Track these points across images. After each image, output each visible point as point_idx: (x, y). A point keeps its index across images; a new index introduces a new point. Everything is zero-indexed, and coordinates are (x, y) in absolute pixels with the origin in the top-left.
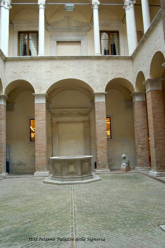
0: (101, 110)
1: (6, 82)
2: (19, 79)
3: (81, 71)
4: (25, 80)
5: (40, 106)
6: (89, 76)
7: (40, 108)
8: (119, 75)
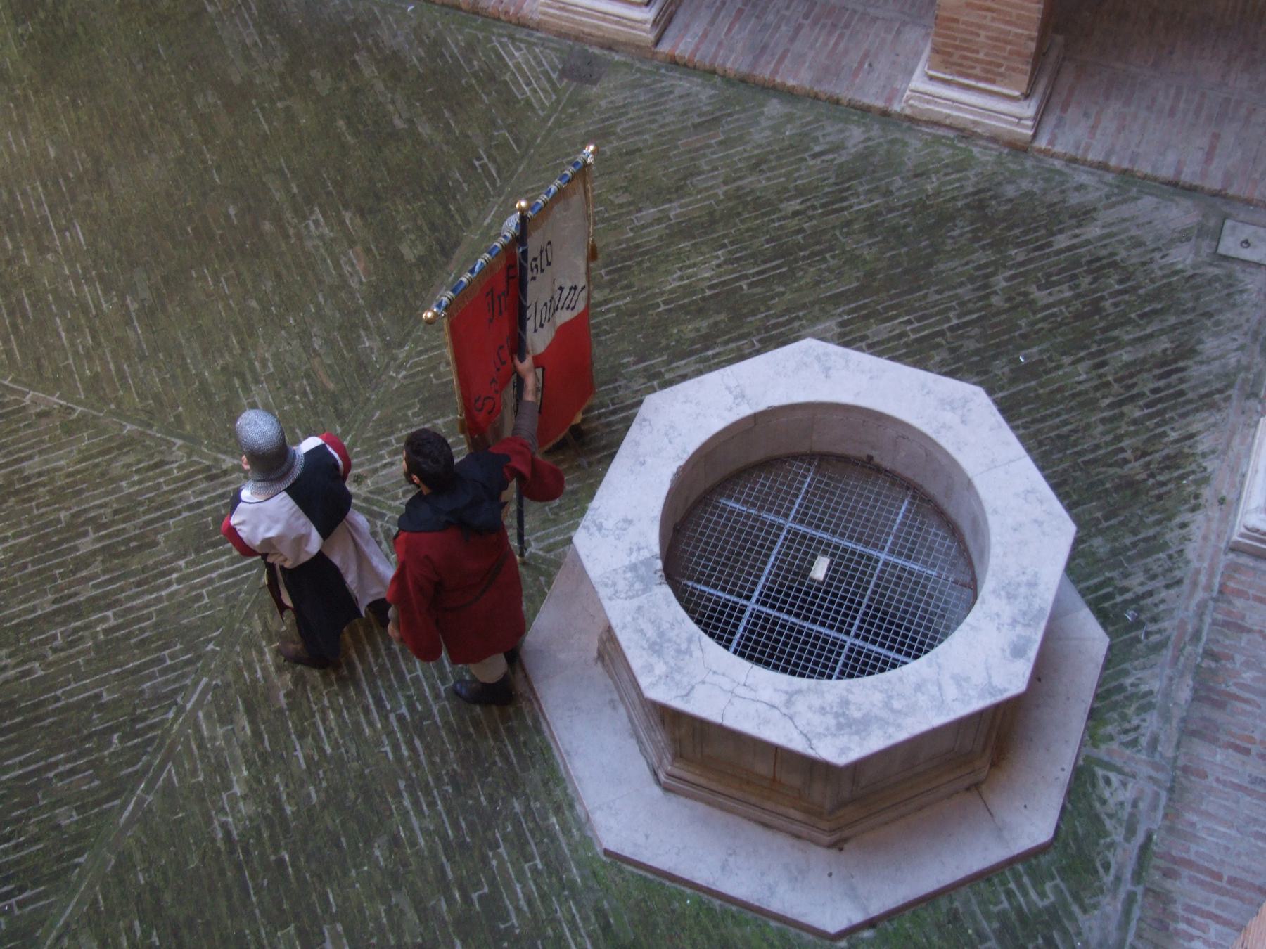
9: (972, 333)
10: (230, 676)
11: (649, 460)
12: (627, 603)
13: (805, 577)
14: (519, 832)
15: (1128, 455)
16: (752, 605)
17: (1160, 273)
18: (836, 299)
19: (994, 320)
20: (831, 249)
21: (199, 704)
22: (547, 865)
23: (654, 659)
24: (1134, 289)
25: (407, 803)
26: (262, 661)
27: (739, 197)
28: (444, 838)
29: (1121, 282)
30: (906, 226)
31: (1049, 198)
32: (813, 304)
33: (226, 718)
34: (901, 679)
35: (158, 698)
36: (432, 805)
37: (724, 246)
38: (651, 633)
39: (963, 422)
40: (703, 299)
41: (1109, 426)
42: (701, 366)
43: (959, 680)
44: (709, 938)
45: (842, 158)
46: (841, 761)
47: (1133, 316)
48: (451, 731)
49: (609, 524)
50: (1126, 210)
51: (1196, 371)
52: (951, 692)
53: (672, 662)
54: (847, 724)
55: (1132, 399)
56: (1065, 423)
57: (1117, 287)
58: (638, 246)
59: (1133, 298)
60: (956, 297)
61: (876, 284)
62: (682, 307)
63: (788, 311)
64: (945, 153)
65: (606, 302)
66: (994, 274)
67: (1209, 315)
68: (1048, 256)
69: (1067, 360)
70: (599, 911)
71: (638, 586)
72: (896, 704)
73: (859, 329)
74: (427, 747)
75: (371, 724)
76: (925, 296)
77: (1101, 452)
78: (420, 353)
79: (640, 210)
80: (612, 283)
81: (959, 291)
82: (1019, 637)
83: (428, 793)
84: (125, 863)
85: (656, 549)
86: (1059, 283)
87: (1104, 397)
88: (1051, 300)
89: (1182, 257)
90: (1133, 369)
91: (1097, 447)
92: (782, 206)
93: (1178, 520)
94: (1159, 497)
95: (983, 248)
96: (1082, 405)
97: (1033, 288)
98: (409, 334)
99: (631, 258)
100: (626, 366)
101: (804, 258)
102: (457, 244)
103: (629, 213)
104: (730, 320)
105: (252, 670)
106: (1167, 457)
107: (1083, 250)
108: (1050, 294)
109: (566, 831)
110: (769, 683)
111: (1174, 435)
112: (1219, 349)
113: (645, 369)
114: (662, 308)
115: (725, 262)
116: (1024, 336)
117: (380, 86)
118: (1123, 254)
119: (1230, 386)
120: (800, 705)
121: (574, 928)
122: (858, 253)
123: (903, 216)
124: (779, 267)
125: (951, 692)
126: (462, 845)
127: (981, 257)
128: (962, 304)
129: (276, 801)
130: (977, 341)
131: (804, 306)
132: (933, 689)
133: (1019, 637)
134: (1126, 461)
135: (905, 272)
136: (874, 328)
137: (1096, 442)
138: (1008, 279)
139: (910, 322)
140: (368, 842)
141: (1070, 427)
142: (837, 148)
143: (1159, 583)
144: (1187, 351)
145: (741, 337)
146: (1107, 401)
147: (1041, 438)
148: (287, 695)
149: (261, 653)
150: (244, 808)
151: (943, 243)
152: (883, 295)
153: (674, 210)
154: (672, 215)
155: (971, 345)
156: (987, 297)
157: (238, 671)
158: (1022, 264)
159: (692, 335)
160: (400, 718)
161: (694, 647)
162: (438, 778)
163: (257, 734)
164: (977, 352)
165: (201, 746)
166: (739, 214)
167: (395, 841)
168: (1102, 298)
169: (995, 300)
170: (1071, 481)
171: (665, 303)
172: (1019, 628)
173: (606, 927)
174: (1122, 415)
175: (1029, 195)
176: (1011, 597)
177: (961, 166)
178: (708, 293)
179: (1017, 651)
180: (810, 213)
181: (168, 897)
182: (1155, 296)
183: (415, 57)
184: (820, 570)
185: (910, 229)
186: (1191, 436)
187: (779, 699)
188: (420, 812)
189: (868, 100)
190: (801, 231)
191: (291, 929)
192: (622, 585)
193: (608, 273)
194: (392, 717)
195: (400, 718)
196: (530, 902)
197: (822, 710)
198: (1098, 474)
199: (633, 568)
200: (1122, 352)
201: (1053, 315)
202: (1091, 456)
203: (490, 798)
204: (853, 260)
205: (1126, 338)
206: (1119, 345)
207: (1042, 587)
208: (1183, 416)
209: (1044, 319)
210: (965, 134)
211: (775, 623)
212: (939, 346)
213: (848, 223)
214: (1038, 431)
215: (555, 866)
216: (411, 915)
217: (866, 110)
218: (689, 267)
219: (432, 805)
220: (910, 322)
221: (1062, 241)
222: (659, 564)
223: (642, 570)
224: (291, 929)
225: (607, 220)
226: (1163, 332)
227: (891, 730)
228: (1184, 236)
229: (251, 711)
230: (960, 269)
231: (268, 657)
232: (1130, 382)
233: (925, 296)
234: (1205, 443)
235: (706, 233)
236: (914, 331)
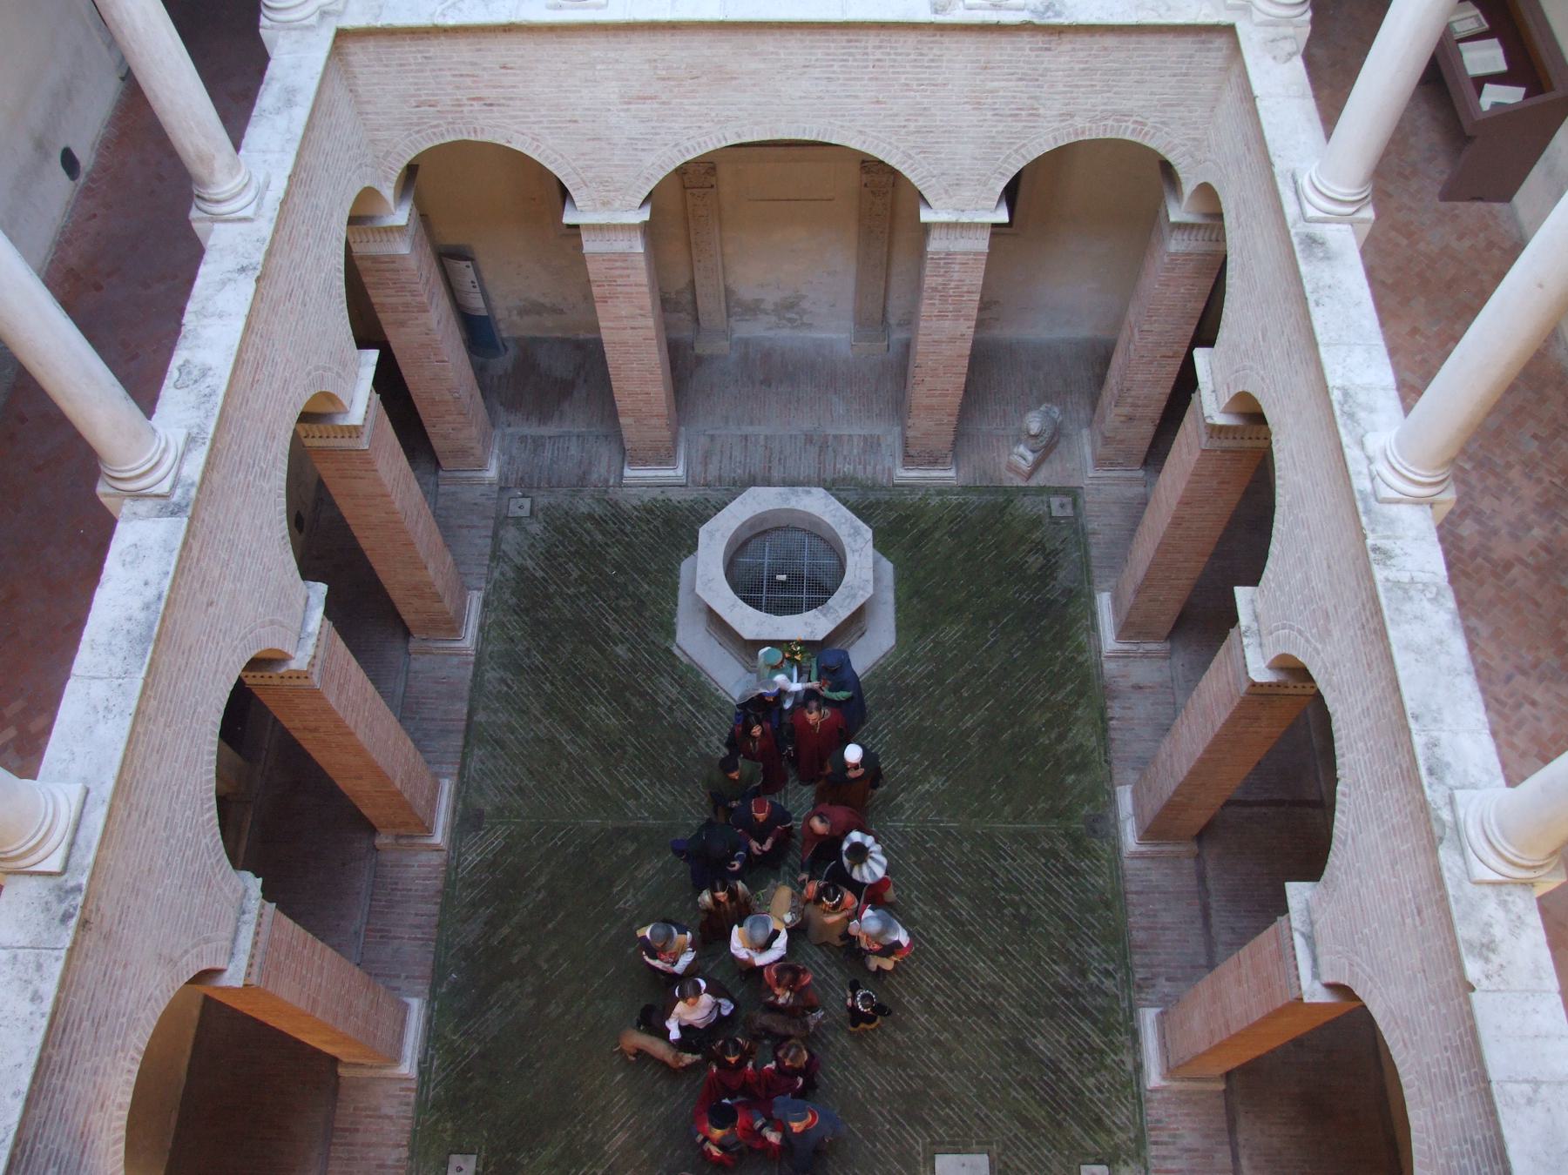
0: (953, 284)
1: (388, 153)
2: (466, 137)
3: (856, 97)
4: (503, 142)
5: (618, 264)
6: (912, 126)
7: (617, 272)
8: (1110, 122)
18: (602, 651)
31: (513, 584)
33: (901, 806)
45: (509, 676)
50: (512, 554)
51: (599, 511)
54: (857, 532)
63: (615, 668)
64: (493, 634)
89: (535, 528)
112: (584, 505)
117: (516, 919)
127: (558, 601)
142: (503, 681)
144: (590, 517)
150: (933, 779)
153: (564, 737)
155: (612, 593)
167: (921, 719)
175: (513, 594)
177: (502, 625)
182: (564, 535)
183: (485, 912)
184: (783, 577)
189: (470, 673)
210: (481, 628)
213: (552, 661)
215: (906, 661)
216: (946, 701)
217: (475, 675)
221: (539, 574)
228: (523, 530)
234: (636, 502)
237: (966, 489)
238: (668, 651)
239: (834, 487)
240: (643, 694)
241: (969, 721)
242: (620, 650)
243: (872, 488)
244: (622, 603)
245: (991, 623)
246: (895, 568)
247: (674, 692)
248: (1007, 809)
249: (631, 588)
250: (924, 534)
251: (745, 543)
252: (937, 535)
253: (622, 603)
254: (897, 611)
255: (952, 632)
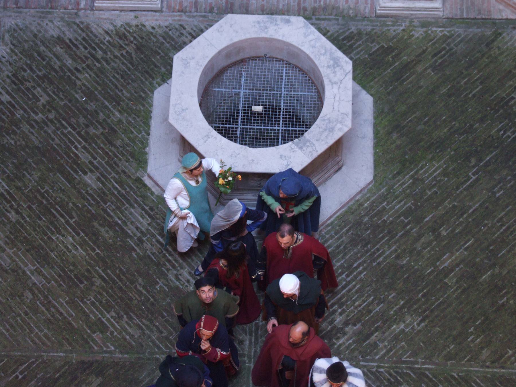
9: (75, 121)
10: (356, 353)
11: (250, 159)
12: (317, 145)
13: (262, 114)
14: (376, 215)
15: (124, 52)
16: (281, 128)
17: (15, 57)
19: (64, 114)
20: (38, 191)
21: (373, 360)
22: (384, 201)
23: (336, 129)
24: (27, 65)
25: (381, 259)
26: (344, 343)
27: (13, 241)
28: (389, 240)
29: (25, 71)
30: (13, 163)
32: (75, 188)
33: (375, 345)
34: (313, 53)
35: (378, 379)
36: (378, 250)
37: (49, 238)
38: (326, 133)
39: (193, 58)
40: (87, 235)
41: (110, 61)
42: (129, 223)
43: (306, 35)
44: (388, 139)
46: (351, 63)
47: (44, 63)
48: (345, 255)
49: (285, 163)
51: (69, 35)
52: (311, 37)
53: (335, 123)
54: (336, 63)
55: (93, 56)
56: (114, 77)
57: (29, 71)
58: (60, 276)
59: (34, 64)
60: (54, 132)
61: (56, 166)
62: (94, 243)
63: (84, 198)
65: (101, 277)
66: (35, 121)
67: (35, 36)
68: (17, 102)
69: (79, 83)
70: (394, 177)
71: (308, 144)
72: (323, 51)
73: (87, 166)
74: (356, 261)
75: (354, 286)
76: (57, 145)
77: (125, 61)
78: (159, 348)
79: (35, 284)
80: (88, 279)
81: (50, 132)
82: (281, 22)
83: (374, 253)
84: (449, 357)
85: (290, 143)
86: (33, 94)
87: (95, 65)
88: (45, 96)
90: (75, 58)
91: (123, 63)
92: (14, 220)
93: (151, 30)
94: (142, 38)
95: (19, 128)
96: (102, 73)
97: (40, 104)
98: (149, 359)
99: (70, 278)
100: (138, 255)
101: (47, 200)
102: (83, 362)
103: (38, 288)
104: (96, 220)
105: (350, 345)
106: (120, 38)
107: (9, 89)
108: (41, 96)
109: (368, 199)
110: (330, 93)
111: (108, 38)
112: (53, 28)
113: (138, 245)
114: (98, 251)
115: (59, 233)
116: (70, 101)
118: (6, 73)
119: (75, 23)
120: (336, 79)
121: (402, 185)
122: (37, 179)
123: (7, 166)
124: (56, 210)
125: (311, 37)
126: (389, 232)
128: (58, 129)
129: (401, 309)
130: (79, 117)
131: (79, 192)
132: (312, 43)
133: (281, 22)
134: (127, 52)
135: (45, 156)
136: (83, 160)
137: (121, 65)
138: (37, 114)
139: (76, 147)
140: (402, 267)
141: (116, 75)
143: (184, 32)
144: (60, 40)
145: (105, 211)
146: (97, 64)
147: (125, 84)
148: (355, 325)
149: (340, 345)
151: (20, 145)
152: (62, 162)
153: (29, 268)
154: (33, 268)
155: (82, 120)
156: (51, 121)
157: (352, 351)
158: (25, 111)
159: (111, 233)
160: (347, 276)
161: (326, 118)
162: (367, 252)
163: (376, 330)
164: (85, 117)
165: (390, 350)
166: (25, 238)
167: (398, 257)
168: (38, 76)
169: (51, 116)
170: (144, 70)
171: (94, 250)
172: (278, 23)
173: (398, 173)
174: (102, 58)
176: (266, 28)
178: (82, 234)
179: (288, 21)
180: (16, 207)
181: (454, 333)
182: (31, 57)
184: (259, 109)
185: (15, 161)
186: (107, 32)
187: (336, 87)
188: (383, 253)
190: (29, 207)
191: (446, 280)
192: (310, 149)
193: (82, 283)
194: (348, 279)
195: (347, 276)
196: (400, 201)
197: (335, 72)
198: (137, 60)
199: (301, 148)
200: (67, 64)
201: (54, 93)
202: (129, 65)
203: (367, 229)
204: (43, 180)
205: (58, 63)
206: (63, 65)
207: (259, 19)
208: (96, 36)
209: (57, 96)
211: (286, 118)
212: (86, 132)
213: (18, 188)
214: (122, 86)
215: (384, 198)
216: (423, 240)
218: (68, 248)
219: (378, 250)
220: (76, 147)
222: (296, 140)
223: (301, 145)
224: (446, 280)
225: (46, 297)
226: (51, 51)
227: (333, 51)
229: (368, 337)
230: (36, 135)
231: (341, 341)
232: (83, 58)
233: (57, 145)
234: (108, 27)
235: (43, 248)
236: (80, 143)
237: (451, 21)
238: (139, 181)
239: (312, 16)
240: (112, 225)
241: (447, 261)
242: (90, 179)
243: (353, 19)
244: (92, 131)
245: (473, 161)
246: (375, 102)
247: (144, 223)
248: (485, 353)
249: (101, 116)
250: (406, 67)
251: (222, 71)
252: (419, 68)
253: (92, 131)
254: (376, 145)
255: (432, 169)
